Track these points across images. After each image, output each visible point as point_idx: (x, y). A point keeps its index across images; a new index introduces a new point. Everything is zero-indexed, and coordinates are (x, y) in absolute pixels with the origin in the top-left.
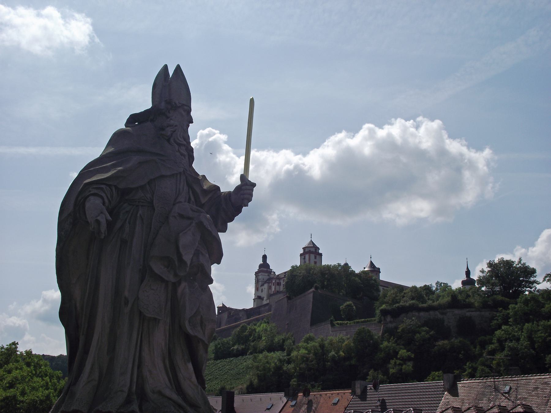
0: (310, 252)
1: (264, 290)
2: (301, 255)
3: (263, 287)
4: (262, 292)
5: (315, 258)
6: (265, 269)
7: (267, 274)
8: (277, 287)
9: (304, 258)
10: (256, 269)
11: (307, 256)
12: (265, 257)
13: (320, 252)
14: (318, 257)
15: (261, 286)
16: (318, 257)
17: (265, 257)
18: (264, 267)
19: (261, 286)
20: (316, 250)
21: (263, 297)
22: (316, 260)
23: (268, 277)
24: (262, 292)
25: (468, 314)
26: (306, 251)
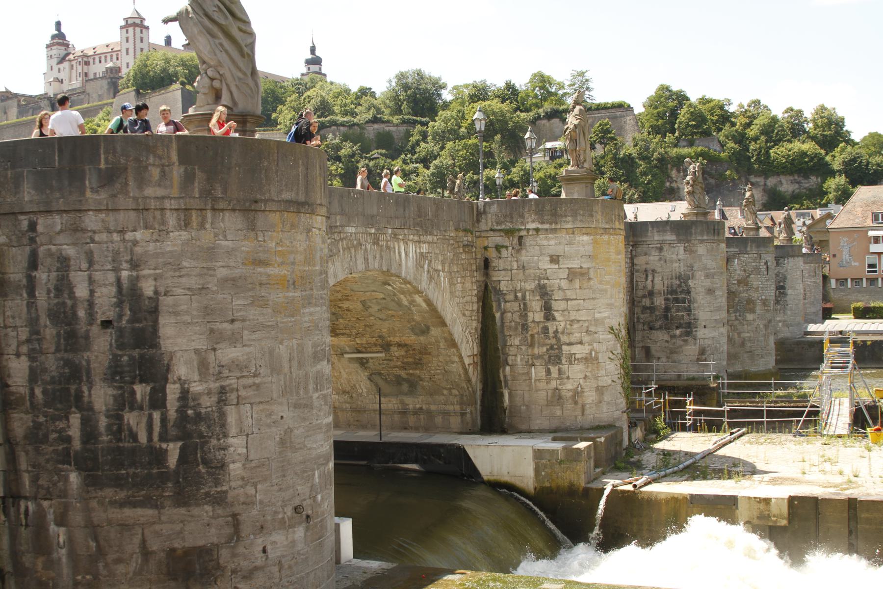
0: (135, 25)
1: (62, 69)
2: (122, 28)
3: (61, 66)
4: (59, 72)
5: (141, 32)
6: (61, 41)
7: (63, 48)
8: (85, 67)
9: (127, 32)
10: (48, 40)
11: (131, 29)
12: (58, 25)
13: (146, 23)
14: (144, 30)
15: (58, 64)
16: (144, 30)
17: (58, 25)
18: (59, 38)
19: (58, 64)
20: (142, 21)
21: (62, 80)
22: (142, 35)
23: (65, 52)
24: (59, 72)
25: (387, 129)
26: (129, 22)
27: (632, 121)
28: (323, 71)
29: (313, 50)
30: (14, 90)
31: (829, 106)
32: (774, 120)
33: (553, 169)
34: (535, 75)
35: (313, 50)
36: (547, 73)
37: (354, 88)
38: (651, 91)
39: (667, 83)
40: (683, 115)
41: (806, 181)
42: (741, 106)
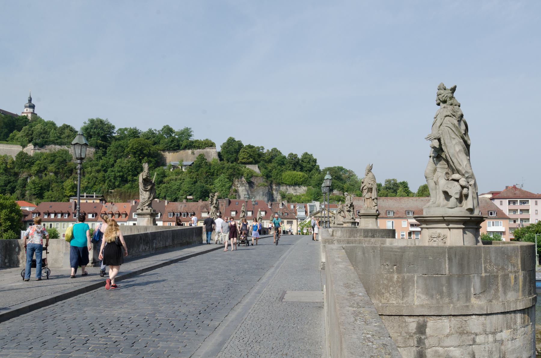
27: (215, 154)
28: (35, 112)
29: (30, 100)
30: (344, 167)
31: (309, 153)
32: (284, 157)
33: (174, 176)
34: (165, 127)
35: (30, 100)
36: (171, 126)
37: (59, 124)
38: (225, 141)
39: (233, 136)
40: (278, 158)
41: (299, 189)
42: (268, 150)
